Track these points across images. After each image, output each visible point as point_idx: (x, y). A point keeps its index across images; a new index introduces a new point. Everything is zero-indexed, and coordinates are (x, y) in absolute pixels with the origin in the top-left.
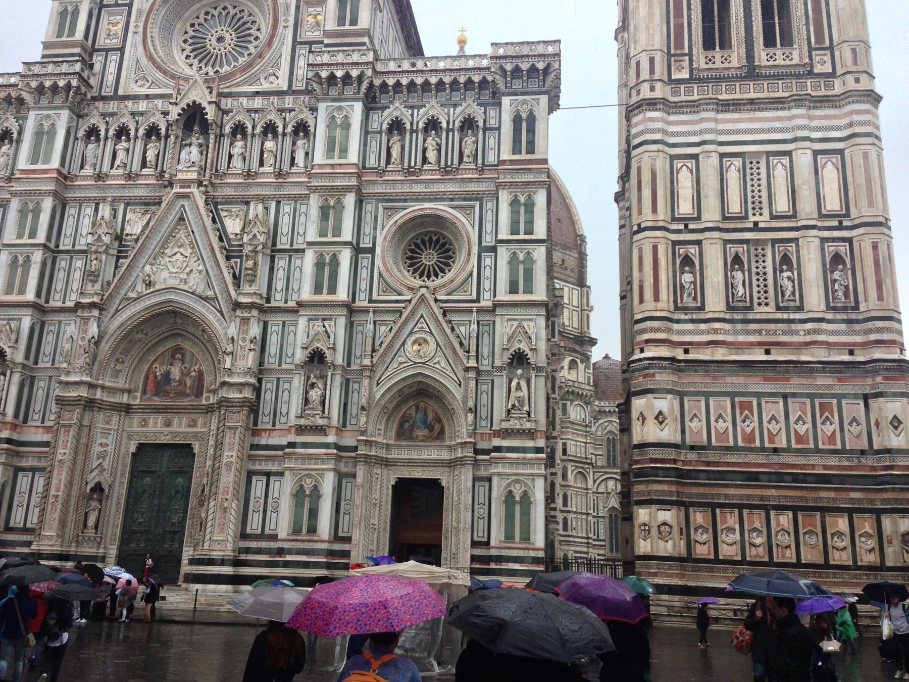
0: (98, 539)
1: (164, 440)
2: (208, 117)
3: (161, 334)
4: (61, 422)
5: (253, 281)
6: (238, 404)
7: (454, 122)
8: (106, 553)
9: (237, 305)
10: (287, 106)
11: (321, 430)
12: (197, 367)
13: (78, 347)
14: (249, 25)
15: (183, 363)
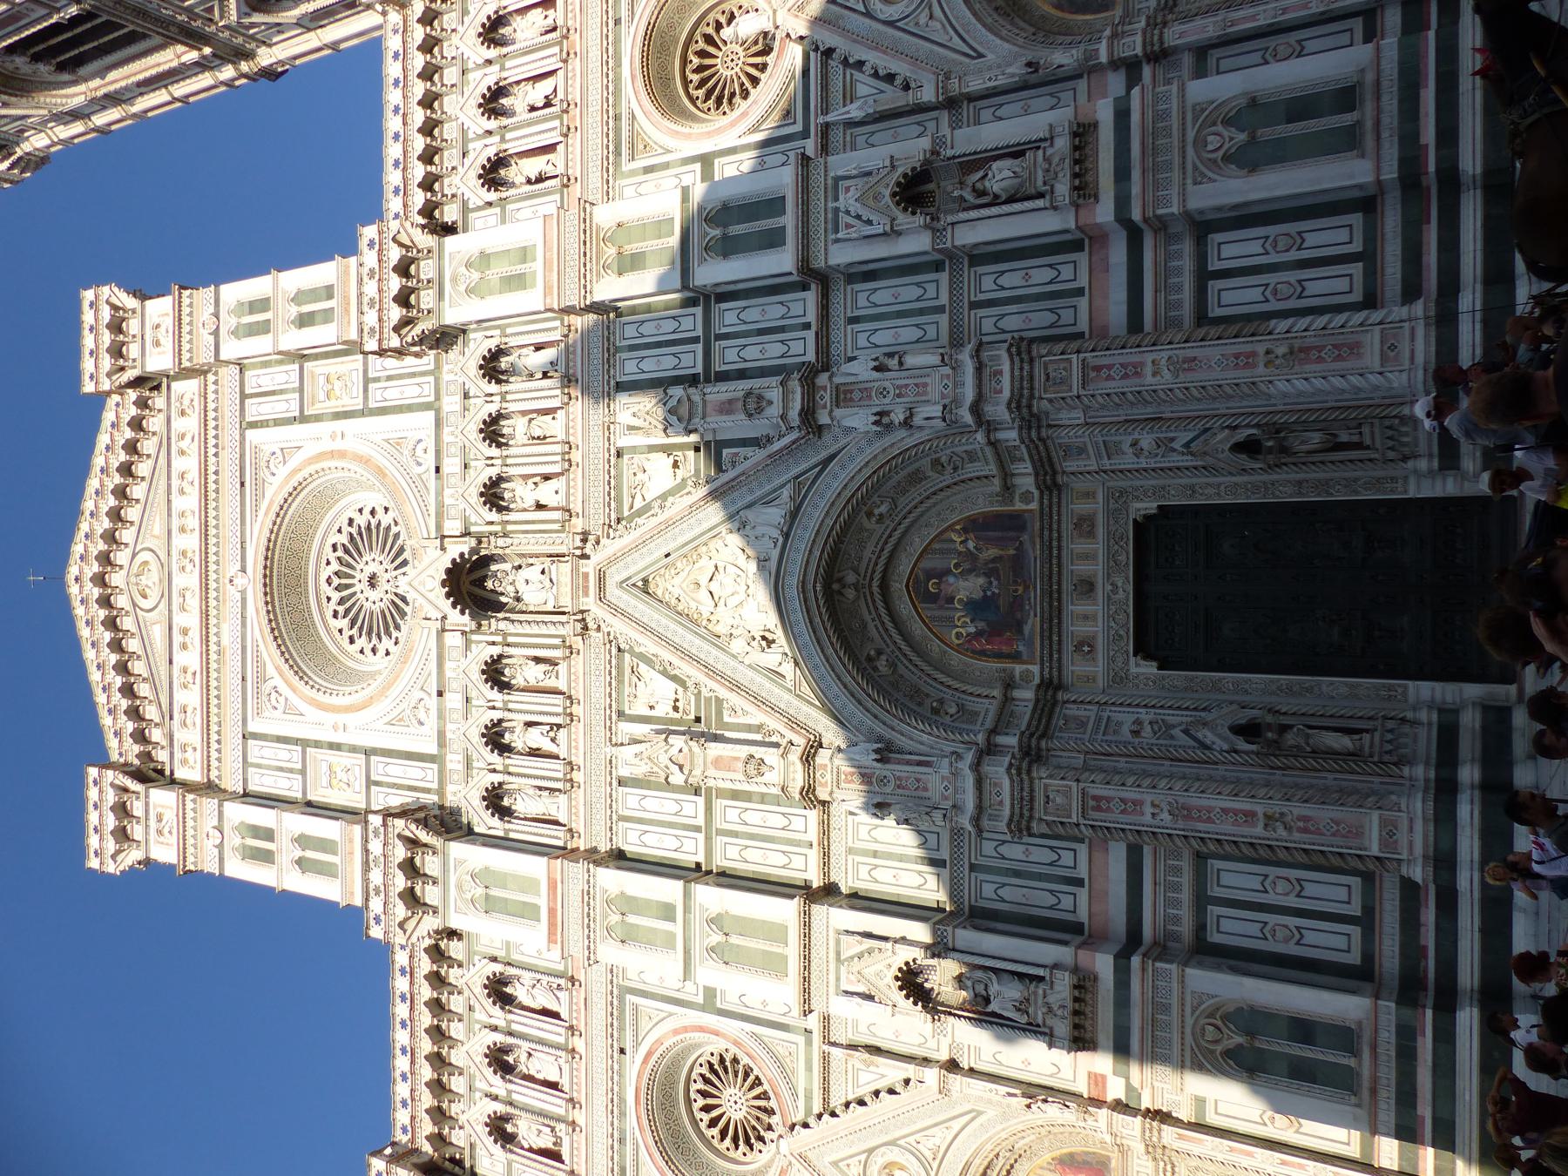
0: (1390, 724)
1: (1130, 588)
2: (466, 549)
3: (883, 623)
4: (1074, 820)
5: (760, 397)
6: (1026, 367)
7: (489, 62)
8: (1430, 708)
9: (808, 414)
10: (457, 408)
11: (1083, 134)
12: (955, 537)
13: (900, 791)
14: (354, 531)
15: (948, 572)
